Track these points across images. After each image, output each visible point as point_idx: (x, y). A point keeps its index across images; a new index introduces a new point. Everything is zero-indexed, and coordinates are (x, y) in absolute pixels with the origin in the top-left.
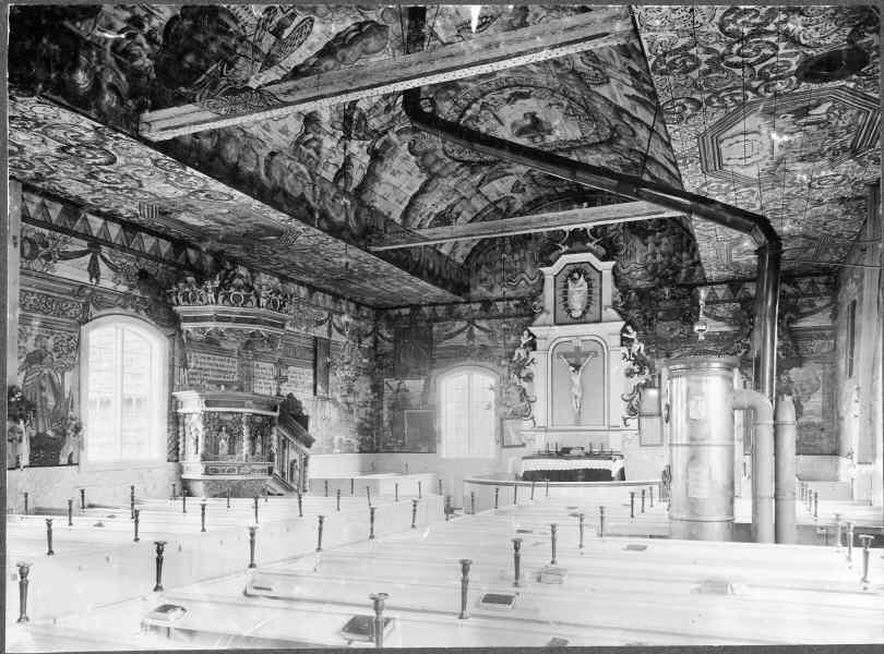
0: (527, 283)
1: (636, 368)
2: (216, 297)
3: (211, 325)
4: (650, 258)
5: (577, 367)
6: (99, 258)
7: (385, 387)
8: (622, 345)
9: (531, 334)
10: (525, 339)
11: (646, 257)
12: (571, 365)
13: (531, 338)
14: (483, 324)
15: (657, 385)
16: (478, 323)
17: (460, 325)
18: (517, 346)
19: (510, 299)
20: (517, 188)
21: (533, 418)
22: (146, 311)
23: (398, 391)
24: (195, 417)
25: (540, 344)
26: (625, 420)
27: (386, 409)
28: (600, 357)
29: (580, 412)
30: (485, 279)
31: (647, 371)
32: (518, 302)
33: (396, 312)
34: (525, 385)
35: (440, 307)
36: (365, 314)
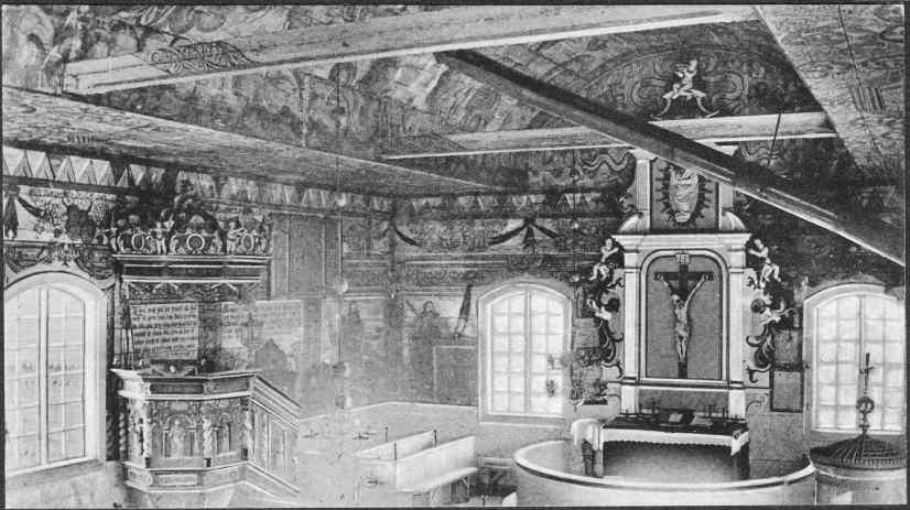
0: (610, 166)
1: (767, 299)
2: (167, 243)
5: (683, 293)
6: (16, 201)
8: (748, 266)
9: (615, 244)
10: (607, 252)
12: (674, 291)
13: (616, 250)
14: (549, 224)
15: (797, 326)
16: (538, 221)
17: (513, 224)
18: (597, 259)
19: (589, 190)
21: (618, 364)
22: (76, 260)
25: (630, 259)
26: (751, 372)
27: (406, 341)
28: (717, 279)
29: (686, 359)
31: (782, 305)
32: (598, 195)
33: (424, 202)
34: (606, 315)
36: (377, 207)
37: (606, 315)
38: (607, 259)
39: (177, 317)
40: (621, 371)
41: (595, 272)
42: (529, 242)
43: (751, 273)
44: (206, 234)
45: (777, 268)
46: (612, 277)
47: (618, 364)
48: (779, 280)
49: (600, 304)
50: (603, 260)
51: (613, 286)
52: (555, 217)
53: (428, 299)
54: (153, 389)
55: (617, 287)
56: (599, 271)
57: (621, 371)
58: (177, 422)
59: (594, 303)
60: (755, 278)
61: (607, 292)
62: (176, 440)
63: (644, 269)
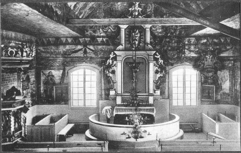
1: (159, 70)
9: (114, 54)
10: (112, 56)
13: (115, 56)
14: (91, 47)
16: (88, 46)
17: (79, 47)
23: (49, 76)
34: (111, 75)
37: (111, 75)
41: (108, 62)
42: (85, 52)
44: (15, 50)
45: (162, 61)
46: (113, 64)
47: (115, 90)
48: (163, 64)
49: (109, 72)
50: (110, 59)
51: (113, 67)
52: (94, 45)
53: (50, 71)
56: (109, 62)
57: (116, 92)
59: (107, 72)
61: (111, 68)
63: (123, 61)
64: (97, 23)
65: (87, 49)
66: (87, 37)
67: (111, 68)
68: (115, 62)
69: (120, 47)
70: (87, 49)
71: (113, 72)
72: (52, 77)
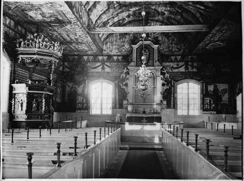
0: (125, 50)
3: (35, 57)
4: (170, 45)
7: (67, 86)
9: (127, 69)
10: (125, 71)
11: (169, 44)
14: (108, 64)
16: (106, 63)
17: (98, 64)
18: (122, 73)
20: (129, 16)
21: (127, 100)
23: (72, 88)
24: (21, 95)
30: (109, 47)
33: (72, 57)
34: (124, 87)
35: (91, 57)
37: (124, 87)
38: (125, 73)
39: (25, 74)
40: (128, 102)
42: (103, 68)
43: (162, 76)
47: (127, 100)
49: (123, 85)
50: (124, 73)
51: (126, 80)
54: (29, 89)
55: (127, 80)
56: (123, 76)
57: (128, 102)
58: (35, 100)
60: (163, 78)
61: (124, 81)
62: (34, 105)
64: (114, 31)
65: (105, 65)
66: (105, 56)
67: (124, 81)
68: (128, 76)
69: (133, 64)
70: (105, 65)
71: (126, 85)
72: (74, 89)
